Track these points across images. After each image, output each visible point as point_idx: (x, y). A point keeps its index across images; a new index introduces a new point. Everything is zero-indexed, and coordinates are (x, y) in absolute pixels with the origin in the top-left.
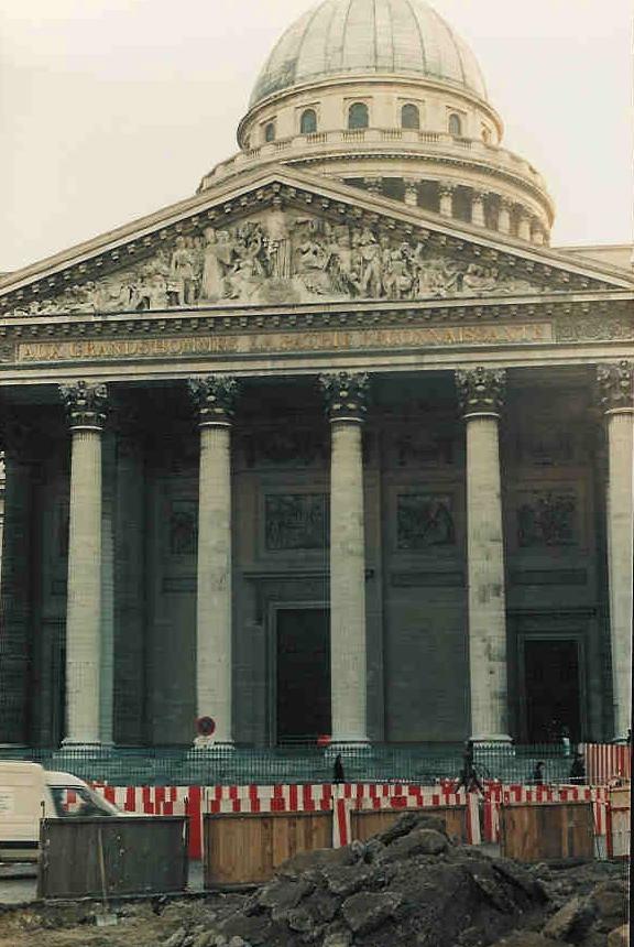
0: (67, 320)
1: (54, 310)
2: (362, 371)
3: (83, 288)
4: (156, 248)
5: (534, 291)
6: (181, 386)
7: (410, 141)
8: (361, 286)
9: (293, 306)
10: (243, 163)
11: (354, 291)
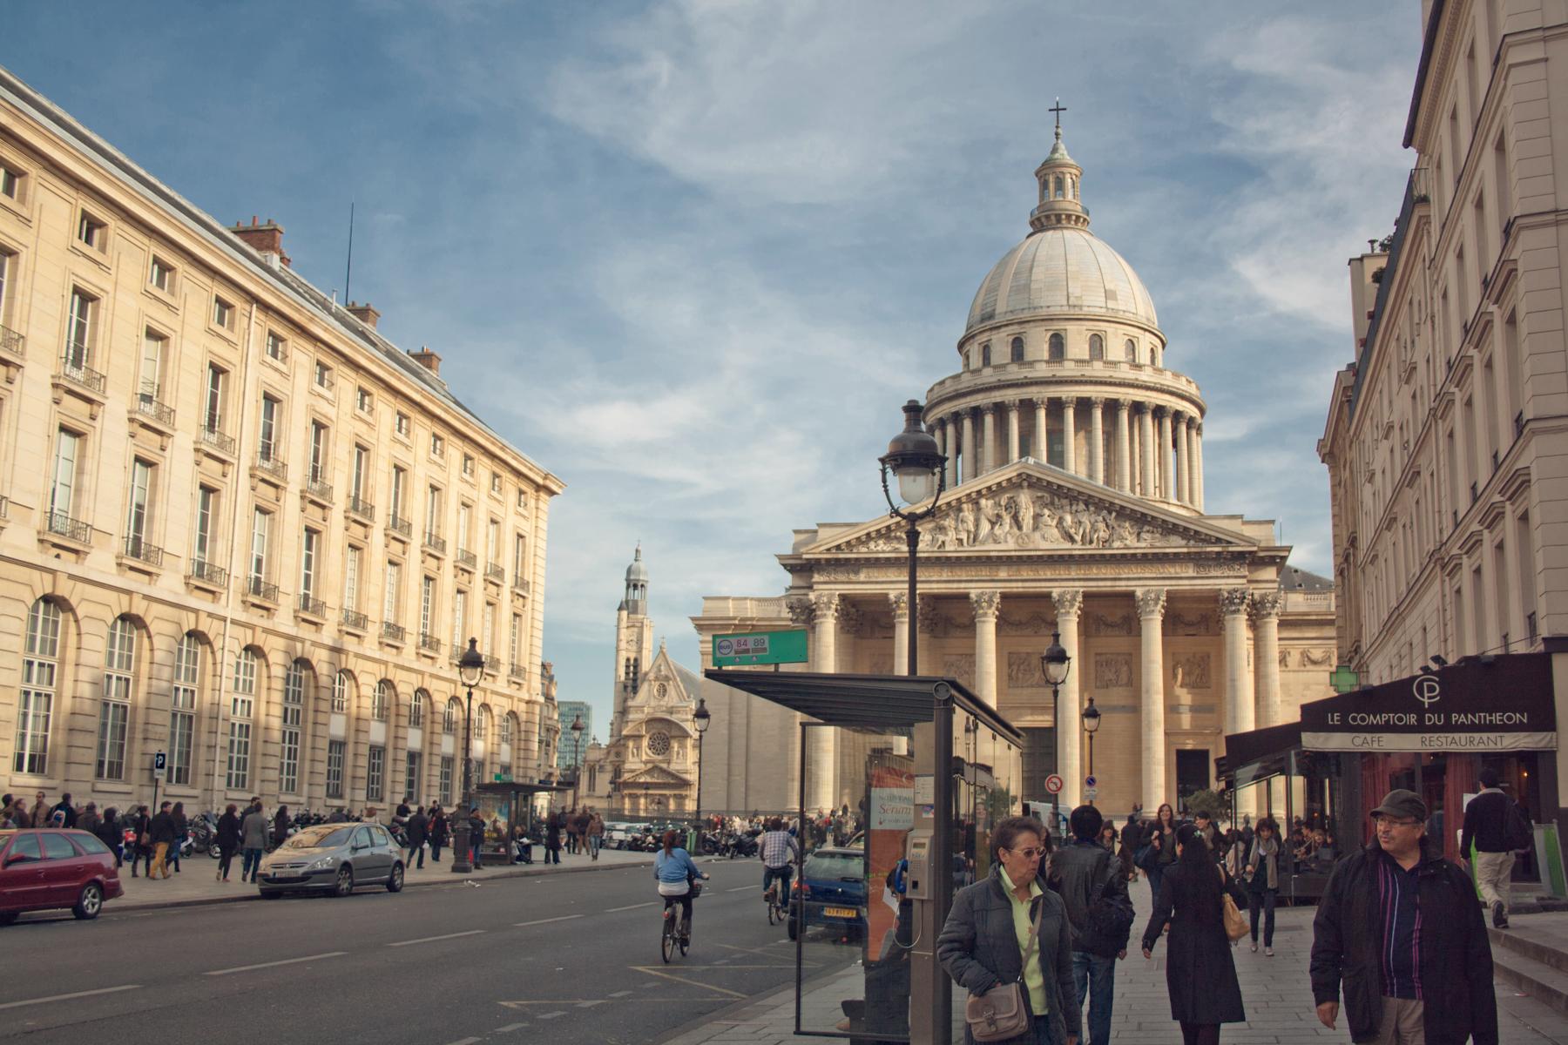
5: (1184, 542)
7: (1097, 370)
8: (1078, 538)
10: (967, 382)
11: (1072, 540)
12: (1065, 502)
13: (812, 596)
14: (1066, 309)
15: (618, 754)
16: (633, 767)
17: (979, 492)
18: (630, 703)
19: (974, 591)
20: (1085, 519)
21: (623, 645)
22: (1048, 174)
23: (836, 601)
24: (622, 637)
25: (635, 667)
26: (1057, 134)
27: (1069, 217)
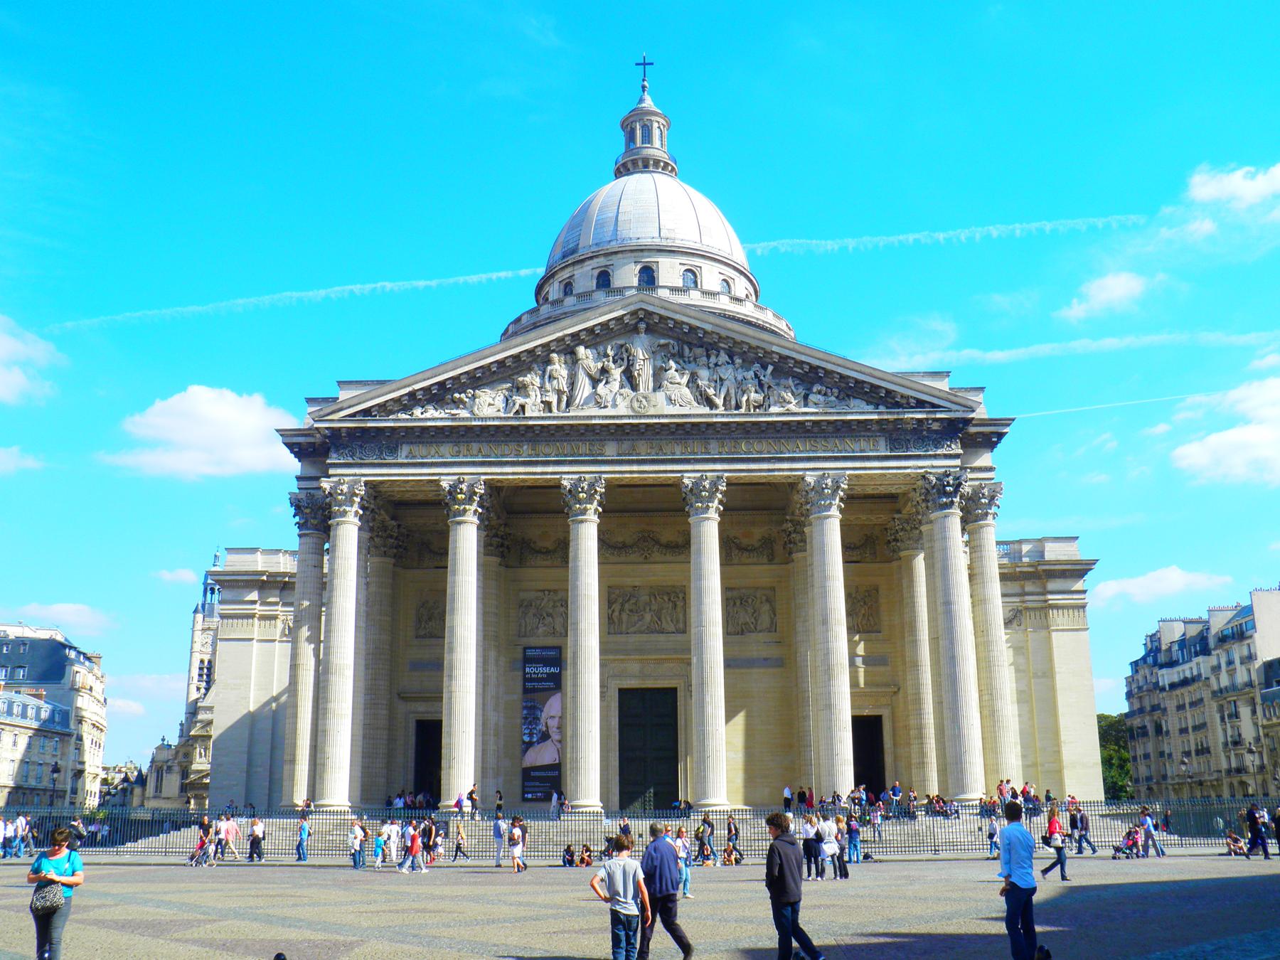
1: (437, 414)
3: (463, 396)
4: (531, 362)
5: (870, 408)
9: (655, 416)
11: (710, 403)
12: (699, 351)
13: (326, 484)
14: (657, 241)
16: (200, 767)
17: (575, 336)
19: (567, 475)
20: (728, 373)
21: (197, 647)
22: (634, 126)
23: (361, 490)
24: (196, 639)
25: (209, 669)
26: (644, 87)
27: (657, 163)
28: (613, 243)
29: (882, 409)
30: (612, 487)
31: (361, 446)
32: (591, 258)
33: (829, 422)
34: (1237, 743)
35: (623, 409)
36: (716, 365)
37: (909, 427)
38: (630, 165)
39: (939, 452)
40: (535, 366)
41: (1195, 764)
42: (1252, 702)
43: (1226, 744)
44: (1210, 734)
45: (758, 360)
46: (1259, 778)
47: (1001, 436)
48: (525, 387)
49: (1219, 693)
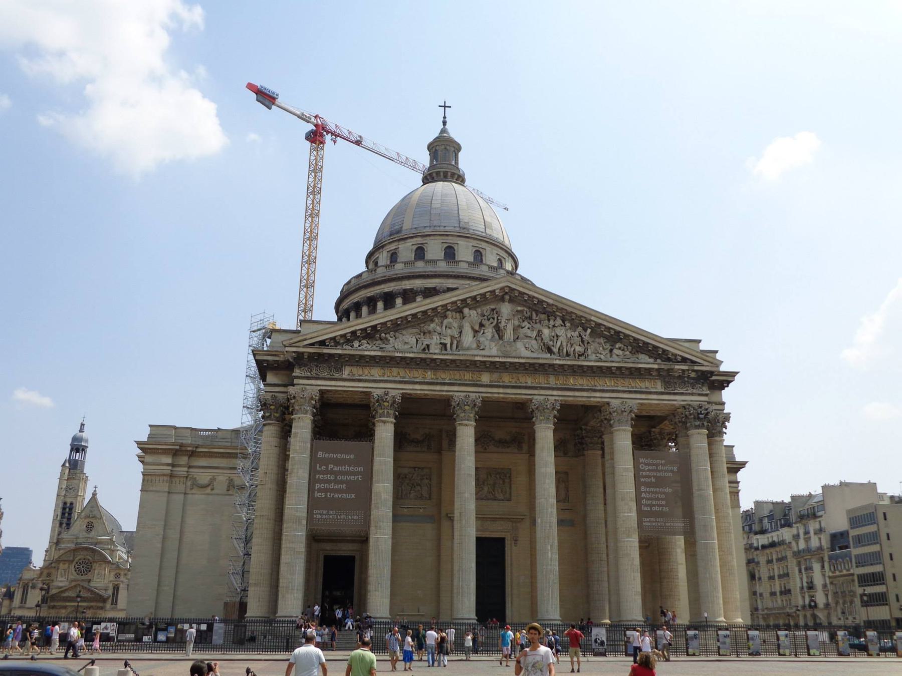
0: (379, 353)
1: (369, 347)
2: (557, 398)
3: (388, 336)
5: (652, 360)
6: (446, 401)
8: (555, 350)
12: (543, 316)
14: (458, 229)
15: (49, 575)
16: (60, 584)
17: (464, 301)
18: (62, 536)
19: (458, 393)
27: (453, 175)
28: (427, 229)
29: (659, 361)
30: (486, 402)
31: (317, 366)
32: (412, 237)
33: (627, 368)
34: (811, 587)
35: (494, 351)
36: (554, 326)
37: (677, 375)
38: (434, 175)
39: (695, 391)
40: (436, 319)
41: (779, 601)
42: (822, 560)
43: (802, 588)
44: (791, 581)
45: (582, 325)
46: (826, 612)
47: (729, 382)
48: (430, 332)
49: (797, 554)
